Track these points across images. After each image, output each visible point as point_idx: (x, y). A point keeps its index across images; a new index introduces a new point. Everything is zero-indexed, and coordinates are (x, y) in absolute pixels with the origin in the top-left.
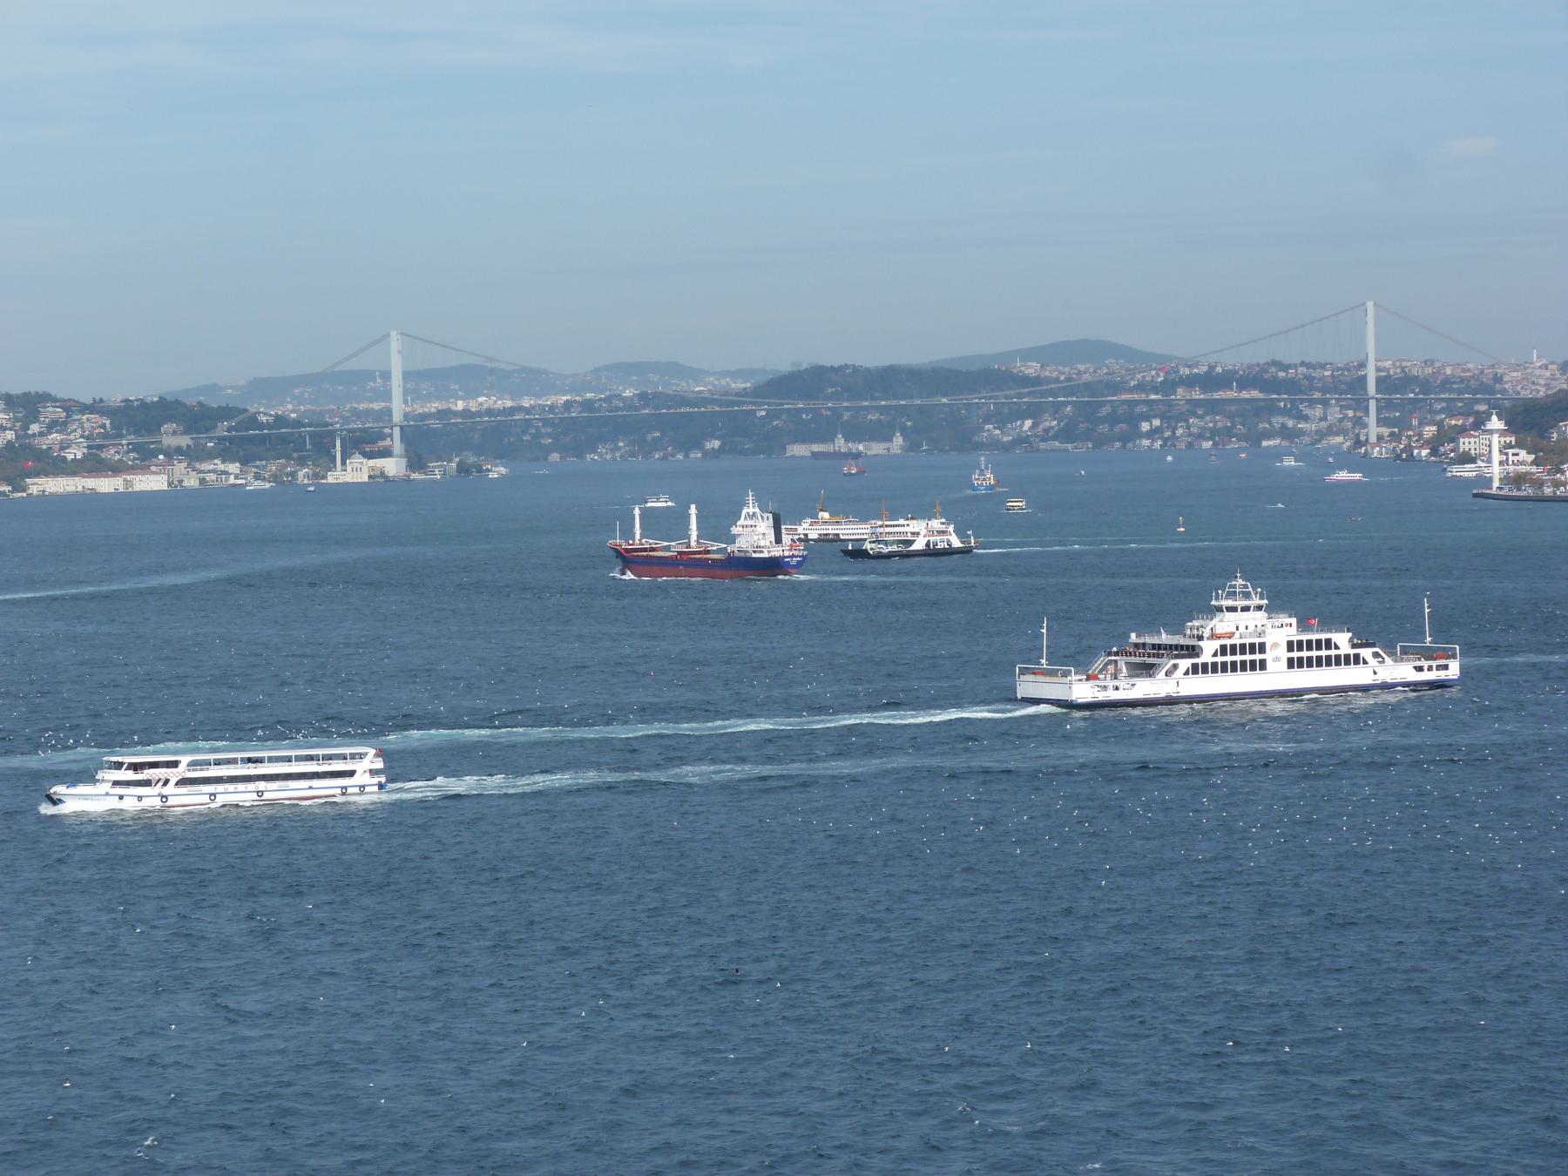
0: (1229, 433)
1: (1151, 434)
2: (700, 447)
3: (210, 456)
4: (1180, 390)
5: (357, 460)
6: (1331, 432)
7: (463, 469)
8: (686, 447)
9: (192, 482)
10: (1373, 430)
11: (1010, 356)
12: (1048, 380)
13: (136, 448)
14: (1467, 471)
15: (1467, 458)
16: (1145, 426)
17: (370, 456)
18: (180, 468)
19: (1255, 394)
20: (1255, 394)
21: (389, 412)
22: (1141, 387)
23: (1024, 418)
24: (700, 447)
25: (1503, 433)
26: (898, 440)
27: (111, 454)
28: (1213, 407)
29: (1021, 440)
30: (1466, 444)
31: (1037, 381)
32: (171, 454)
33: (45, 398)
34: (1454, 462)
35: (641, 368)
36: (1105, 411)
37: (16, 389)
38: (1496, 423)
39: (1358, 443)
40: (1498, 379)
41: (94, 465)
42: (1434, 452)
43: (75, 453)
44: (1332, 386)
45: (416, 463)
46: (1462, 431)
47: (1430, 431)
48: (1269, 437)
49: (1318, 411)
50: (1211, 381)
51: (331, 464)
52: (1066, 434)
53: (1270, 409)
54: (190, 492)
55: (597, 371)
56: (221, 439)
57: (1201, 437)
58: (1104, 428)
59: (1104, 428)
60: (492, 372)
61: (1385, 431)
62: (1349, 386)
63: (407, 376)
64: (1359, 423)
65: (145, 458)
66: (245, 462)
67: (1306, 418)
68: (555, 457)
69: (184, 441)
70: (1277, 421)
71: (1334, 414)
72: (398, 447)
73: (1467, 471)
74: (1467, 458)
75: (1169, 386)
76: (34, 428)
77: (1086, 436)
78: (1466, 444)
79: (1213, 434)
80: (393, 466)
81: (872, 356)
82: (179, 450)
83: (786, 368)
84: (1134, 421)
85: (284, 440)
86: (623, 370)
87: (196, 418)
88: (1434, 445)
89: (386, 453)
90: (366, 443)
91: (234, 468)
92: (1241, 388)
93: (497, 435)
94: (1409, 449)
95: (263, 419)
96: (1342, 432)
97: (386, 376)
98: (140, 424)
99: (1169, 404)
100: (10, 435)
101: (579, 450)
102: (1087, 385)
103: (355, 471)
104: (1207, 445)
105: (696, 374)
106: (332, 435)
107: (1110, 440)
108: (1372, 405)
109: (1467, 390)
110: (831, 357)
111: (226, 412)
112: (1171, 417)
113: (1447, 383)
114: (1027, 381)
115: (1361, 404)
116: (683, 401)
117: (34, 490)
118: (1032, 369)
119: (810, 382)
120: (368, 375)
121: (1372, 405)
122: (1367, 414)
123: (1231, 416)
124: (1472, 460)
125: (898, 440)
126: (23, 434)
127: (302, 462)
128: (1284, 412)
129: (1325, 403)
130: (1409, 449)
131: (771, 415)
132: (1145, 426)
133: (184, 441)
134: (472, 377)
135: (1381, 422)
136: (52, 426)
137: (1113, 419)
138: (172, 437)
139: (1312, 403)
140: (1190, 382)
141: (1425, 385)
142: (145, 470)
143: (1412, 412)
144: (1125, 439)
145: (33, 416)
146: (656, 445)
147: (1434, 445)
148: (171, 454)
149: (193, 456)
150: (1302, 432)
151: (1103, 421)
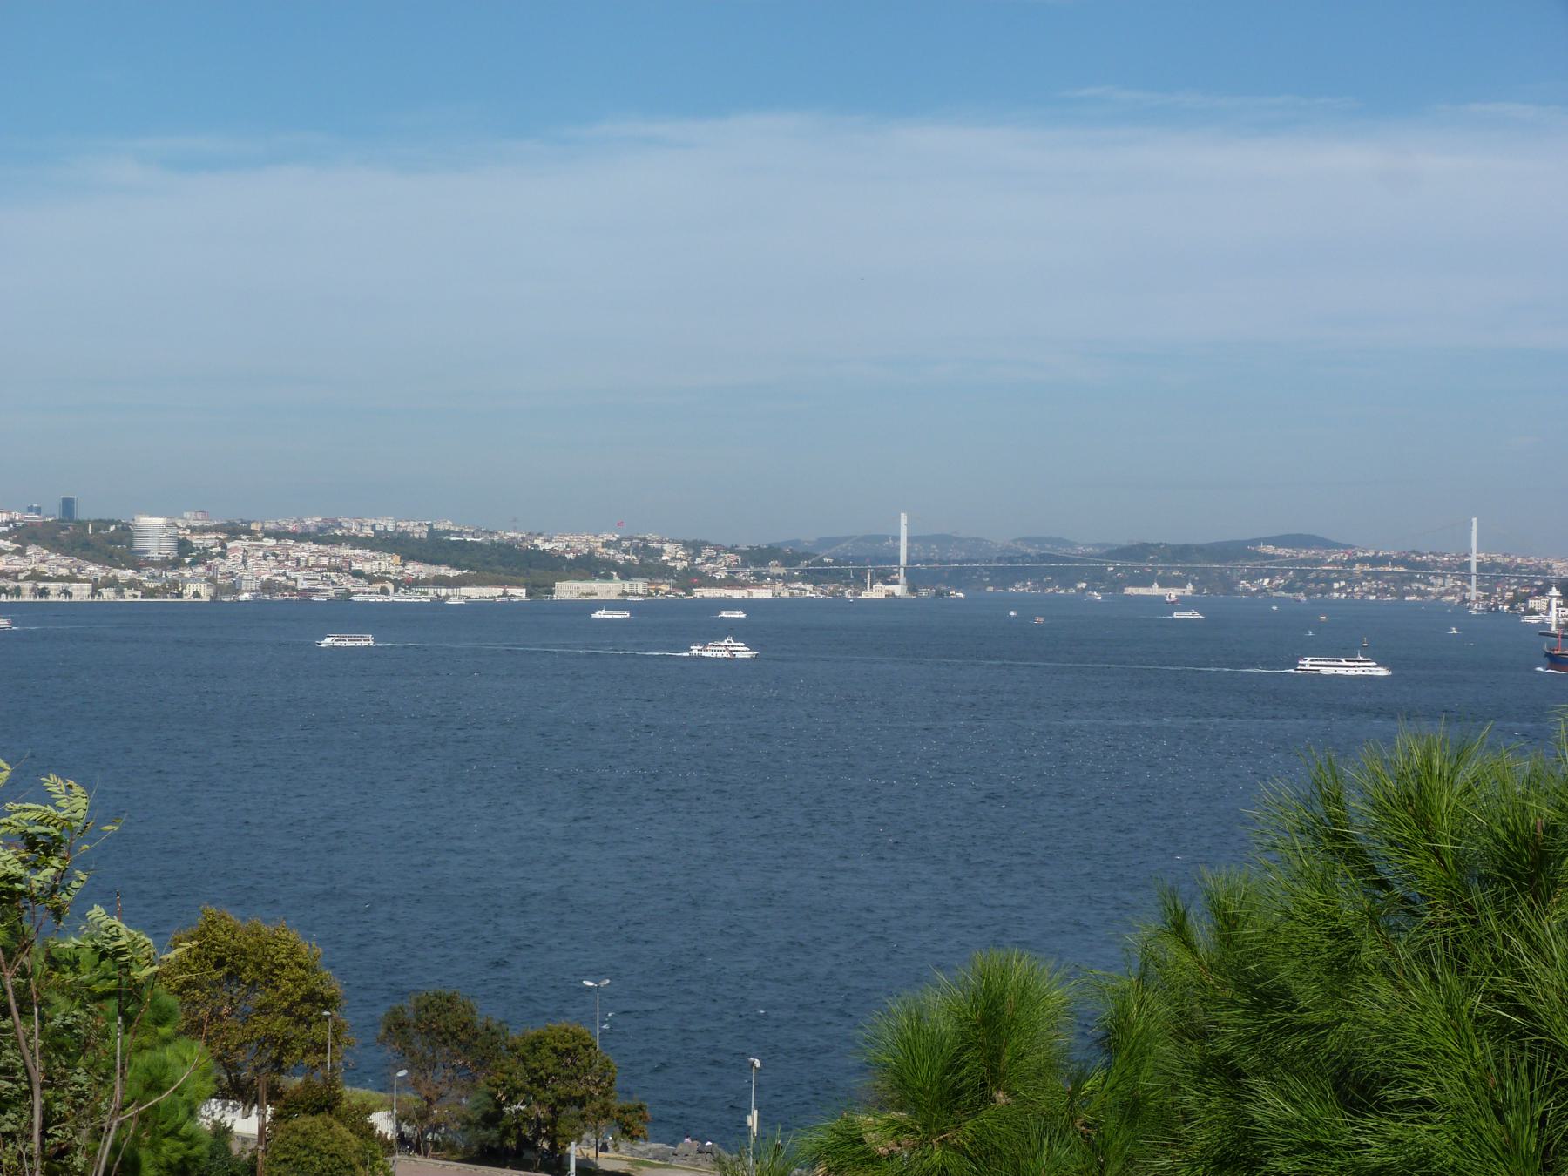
0: (1385, 591)
1: (1339, 590)
2: (1074, 587)
3: (796, 580)
4: (1358, 567)
5: (879, 586)
6: (1447, 593)
7: (939, 594)
8: (1067, 586)
9: (785, 594)
10: (1473, 593)
11: (1256, 542)
12: (1279, 556)
13: (755, 574)
14: (1534, 620)
15: (1533, 612)
16: (1336, 585)
17: (887, 583)
18: (779, 585)
19: (1402, 569)
20: (1402, 569)
21: (896, 560)
22: (1334, 563)
23: (1264, 577)
24: (1074, 587)
25: (1559, 598)
26: (1190, 587)
27: (740, 576)
28: (1377, 576)
29: (1262, 590)
30: (1532, 604)
31: (1273, 557)
32: (775, 578)
33: (705, 544)
34: (1524, 614)
35: (1040, 541)
36: (1312, 576)
37: (690, 538)
38: (1555, 592)
39: (1464, 600)
40: (1550, 567)
41: (731, 582)
42: (1512, 608)
43: (721, 575)
44: (1448, 568)
45: (912, 589)
46: (1529, 596)
47: (1509, 595)
48: (1409, 593)
49: (1440, 581)
50: (1375, 561)
51: (864, 589)
52: (1288, 588)
53: (1412, 579)
54: (785, 600)
55: (1015, 541)
56: (802, 571)
57: (1369, 593)
58: (1311, 586)
59: (1311, 586)
60: (956, 539)
61: (1481, 594)
62: (1461, 569)
63: (909, 539)
64: (1463, 588)
65: (760, 580)
66: (815, 584)
67: (1432, 585)
68: (990, 589)
69: (782, 571)
70: (1415, 585)
71: (1449, 583)
72: (902, 579)
73: (1534, 620)
74: (1533, 612)
75: (1351, 562)
76: (699, 560)
77: (1299, 590)
78: (1532, 604)
79: (1377, 591)
80: (899, 590)
81: (1177, 539)
82: (779, 576)
83: (1125, 543)
84: (1330, 582)
85: (838, 572)
86: (1028, 541)
87: (789, 560)
88: (1512, 603)
89: (895, 582)
90: (886, 578)
91: (809, 587)
92: (1394, 565)
93: (959, 577)
94: (1496, 605)
95: (826, 560)
96: (1455, 593)
97: (897, 539)
98: (758, 559)
99: (1351, 573)
100: (685, 564)
101: (1005, 585)
102: (1303, 562)
103: (878, 592)
104: (1373, 598)
105: (1071, 545)
106: (865, 571)
107: (1316, 592)
108: (1474, 578)
109: (1530, 572)
110: (1152, 539)
111: (806, 556)
112: (1352, 581)
113: (1518, 566)
114: (1267, 556)
115: (1466, 578)
116: (1066, 560)
117: (697, 595)
118: (1270, 550)
119: (1137, 552)
120: (886, 538)
121: (1474, 578)
122: (1470, 582)
123: (1387, 581)
124: (1537, 613)
125: (1190, 587)
126: (692, 564)
127: (847, 586)
128: (1419, 581)
129: (1444, 576)
130: (1496, 605)
131: (1117, 570)
132: (1336, 585)
133: (782, 571)
134: (943, 540)
135: (1479, 589)
136: (708, 559)
137: (1317, 581)
138: (775, 568)
139: (1436, 576)
140: (1363, 561)
141: (1505, 568)
142: (759, 586)
143: (1497, 585)
144: (1323, 592)
145: (698, 554)
146: (1049, 584)
147: (1512, 603)
148: (775, 578)
149: (787, 579)
150: (1430, 593)
151: (1309, 581)
